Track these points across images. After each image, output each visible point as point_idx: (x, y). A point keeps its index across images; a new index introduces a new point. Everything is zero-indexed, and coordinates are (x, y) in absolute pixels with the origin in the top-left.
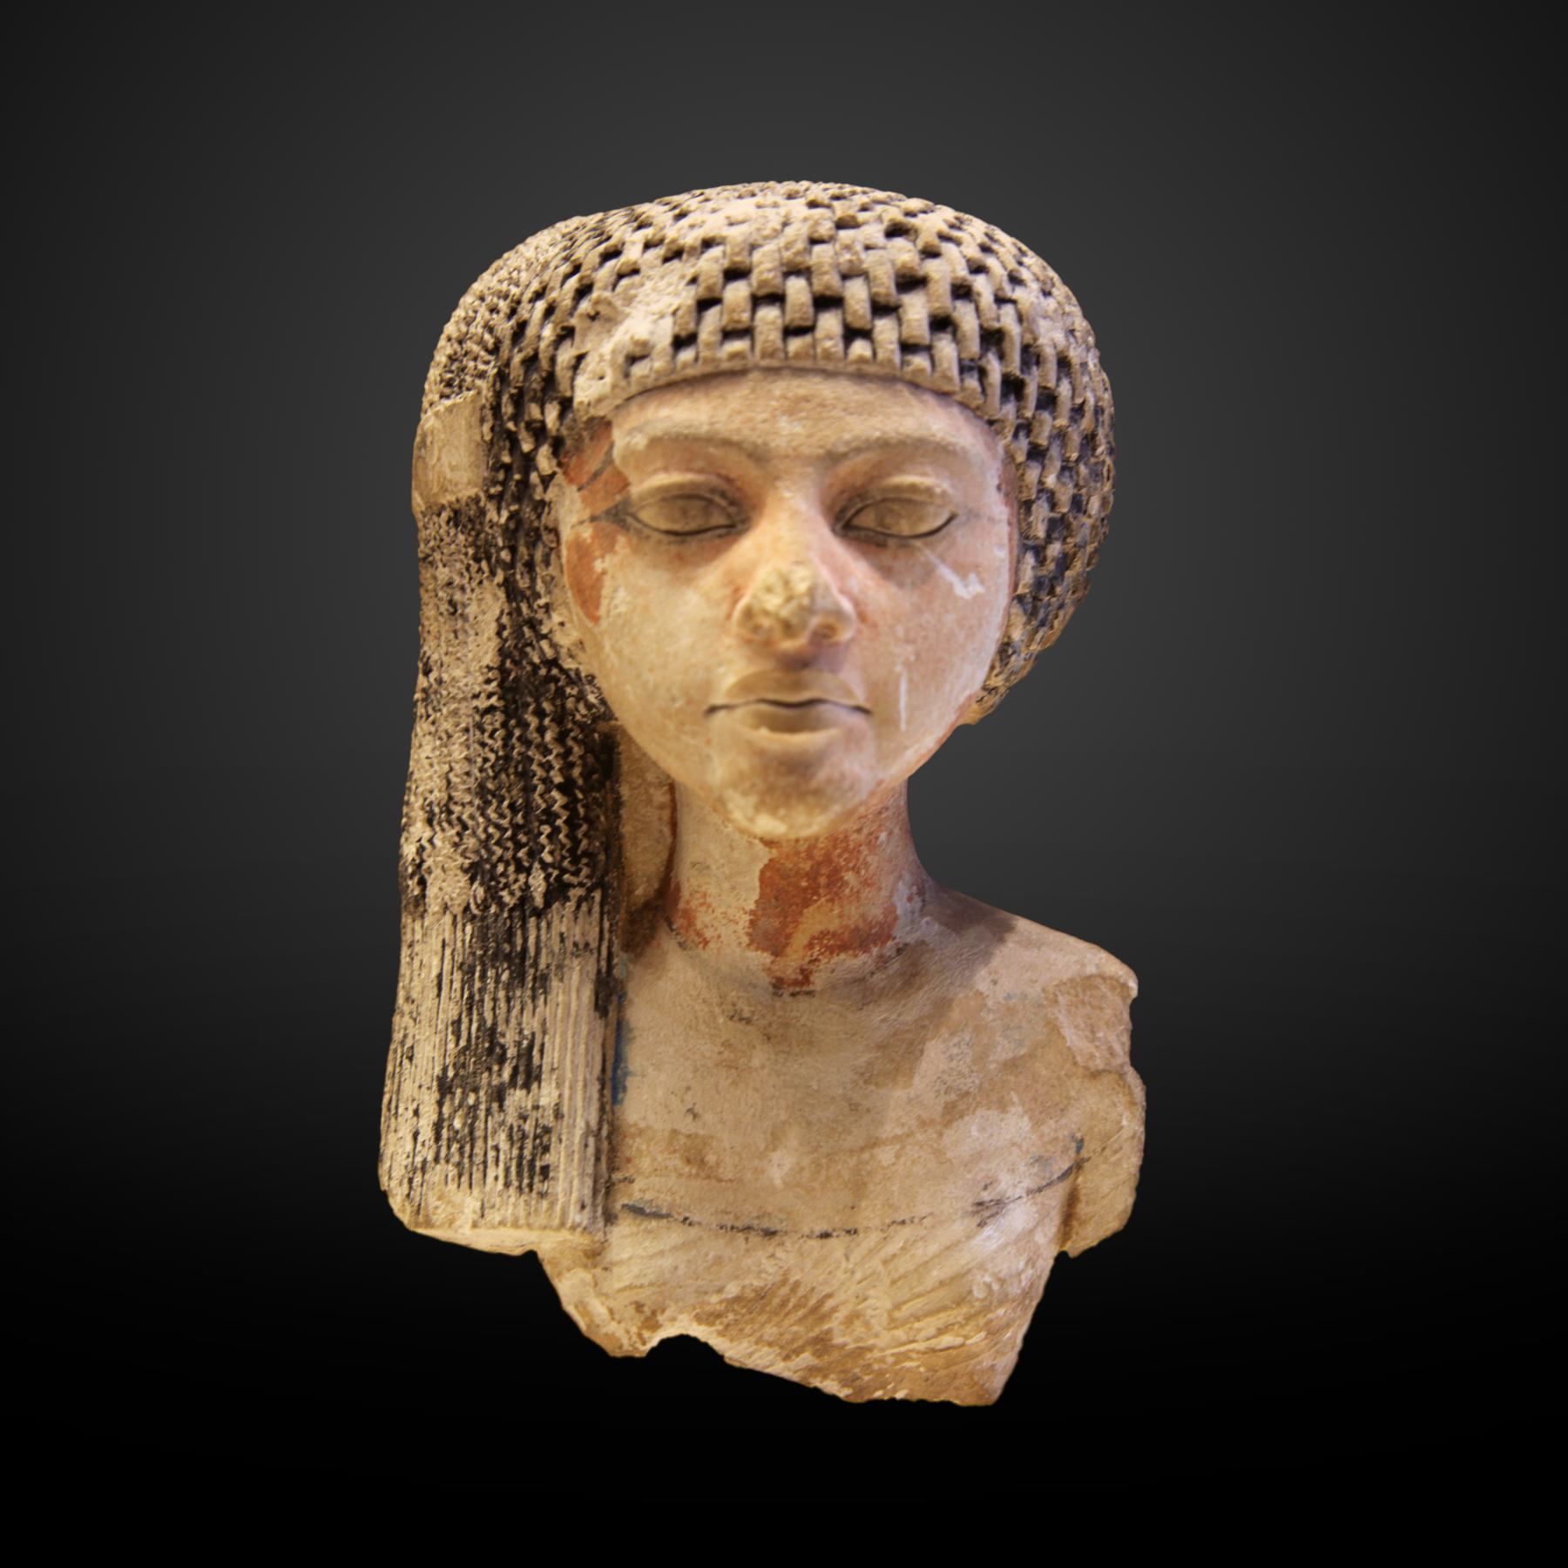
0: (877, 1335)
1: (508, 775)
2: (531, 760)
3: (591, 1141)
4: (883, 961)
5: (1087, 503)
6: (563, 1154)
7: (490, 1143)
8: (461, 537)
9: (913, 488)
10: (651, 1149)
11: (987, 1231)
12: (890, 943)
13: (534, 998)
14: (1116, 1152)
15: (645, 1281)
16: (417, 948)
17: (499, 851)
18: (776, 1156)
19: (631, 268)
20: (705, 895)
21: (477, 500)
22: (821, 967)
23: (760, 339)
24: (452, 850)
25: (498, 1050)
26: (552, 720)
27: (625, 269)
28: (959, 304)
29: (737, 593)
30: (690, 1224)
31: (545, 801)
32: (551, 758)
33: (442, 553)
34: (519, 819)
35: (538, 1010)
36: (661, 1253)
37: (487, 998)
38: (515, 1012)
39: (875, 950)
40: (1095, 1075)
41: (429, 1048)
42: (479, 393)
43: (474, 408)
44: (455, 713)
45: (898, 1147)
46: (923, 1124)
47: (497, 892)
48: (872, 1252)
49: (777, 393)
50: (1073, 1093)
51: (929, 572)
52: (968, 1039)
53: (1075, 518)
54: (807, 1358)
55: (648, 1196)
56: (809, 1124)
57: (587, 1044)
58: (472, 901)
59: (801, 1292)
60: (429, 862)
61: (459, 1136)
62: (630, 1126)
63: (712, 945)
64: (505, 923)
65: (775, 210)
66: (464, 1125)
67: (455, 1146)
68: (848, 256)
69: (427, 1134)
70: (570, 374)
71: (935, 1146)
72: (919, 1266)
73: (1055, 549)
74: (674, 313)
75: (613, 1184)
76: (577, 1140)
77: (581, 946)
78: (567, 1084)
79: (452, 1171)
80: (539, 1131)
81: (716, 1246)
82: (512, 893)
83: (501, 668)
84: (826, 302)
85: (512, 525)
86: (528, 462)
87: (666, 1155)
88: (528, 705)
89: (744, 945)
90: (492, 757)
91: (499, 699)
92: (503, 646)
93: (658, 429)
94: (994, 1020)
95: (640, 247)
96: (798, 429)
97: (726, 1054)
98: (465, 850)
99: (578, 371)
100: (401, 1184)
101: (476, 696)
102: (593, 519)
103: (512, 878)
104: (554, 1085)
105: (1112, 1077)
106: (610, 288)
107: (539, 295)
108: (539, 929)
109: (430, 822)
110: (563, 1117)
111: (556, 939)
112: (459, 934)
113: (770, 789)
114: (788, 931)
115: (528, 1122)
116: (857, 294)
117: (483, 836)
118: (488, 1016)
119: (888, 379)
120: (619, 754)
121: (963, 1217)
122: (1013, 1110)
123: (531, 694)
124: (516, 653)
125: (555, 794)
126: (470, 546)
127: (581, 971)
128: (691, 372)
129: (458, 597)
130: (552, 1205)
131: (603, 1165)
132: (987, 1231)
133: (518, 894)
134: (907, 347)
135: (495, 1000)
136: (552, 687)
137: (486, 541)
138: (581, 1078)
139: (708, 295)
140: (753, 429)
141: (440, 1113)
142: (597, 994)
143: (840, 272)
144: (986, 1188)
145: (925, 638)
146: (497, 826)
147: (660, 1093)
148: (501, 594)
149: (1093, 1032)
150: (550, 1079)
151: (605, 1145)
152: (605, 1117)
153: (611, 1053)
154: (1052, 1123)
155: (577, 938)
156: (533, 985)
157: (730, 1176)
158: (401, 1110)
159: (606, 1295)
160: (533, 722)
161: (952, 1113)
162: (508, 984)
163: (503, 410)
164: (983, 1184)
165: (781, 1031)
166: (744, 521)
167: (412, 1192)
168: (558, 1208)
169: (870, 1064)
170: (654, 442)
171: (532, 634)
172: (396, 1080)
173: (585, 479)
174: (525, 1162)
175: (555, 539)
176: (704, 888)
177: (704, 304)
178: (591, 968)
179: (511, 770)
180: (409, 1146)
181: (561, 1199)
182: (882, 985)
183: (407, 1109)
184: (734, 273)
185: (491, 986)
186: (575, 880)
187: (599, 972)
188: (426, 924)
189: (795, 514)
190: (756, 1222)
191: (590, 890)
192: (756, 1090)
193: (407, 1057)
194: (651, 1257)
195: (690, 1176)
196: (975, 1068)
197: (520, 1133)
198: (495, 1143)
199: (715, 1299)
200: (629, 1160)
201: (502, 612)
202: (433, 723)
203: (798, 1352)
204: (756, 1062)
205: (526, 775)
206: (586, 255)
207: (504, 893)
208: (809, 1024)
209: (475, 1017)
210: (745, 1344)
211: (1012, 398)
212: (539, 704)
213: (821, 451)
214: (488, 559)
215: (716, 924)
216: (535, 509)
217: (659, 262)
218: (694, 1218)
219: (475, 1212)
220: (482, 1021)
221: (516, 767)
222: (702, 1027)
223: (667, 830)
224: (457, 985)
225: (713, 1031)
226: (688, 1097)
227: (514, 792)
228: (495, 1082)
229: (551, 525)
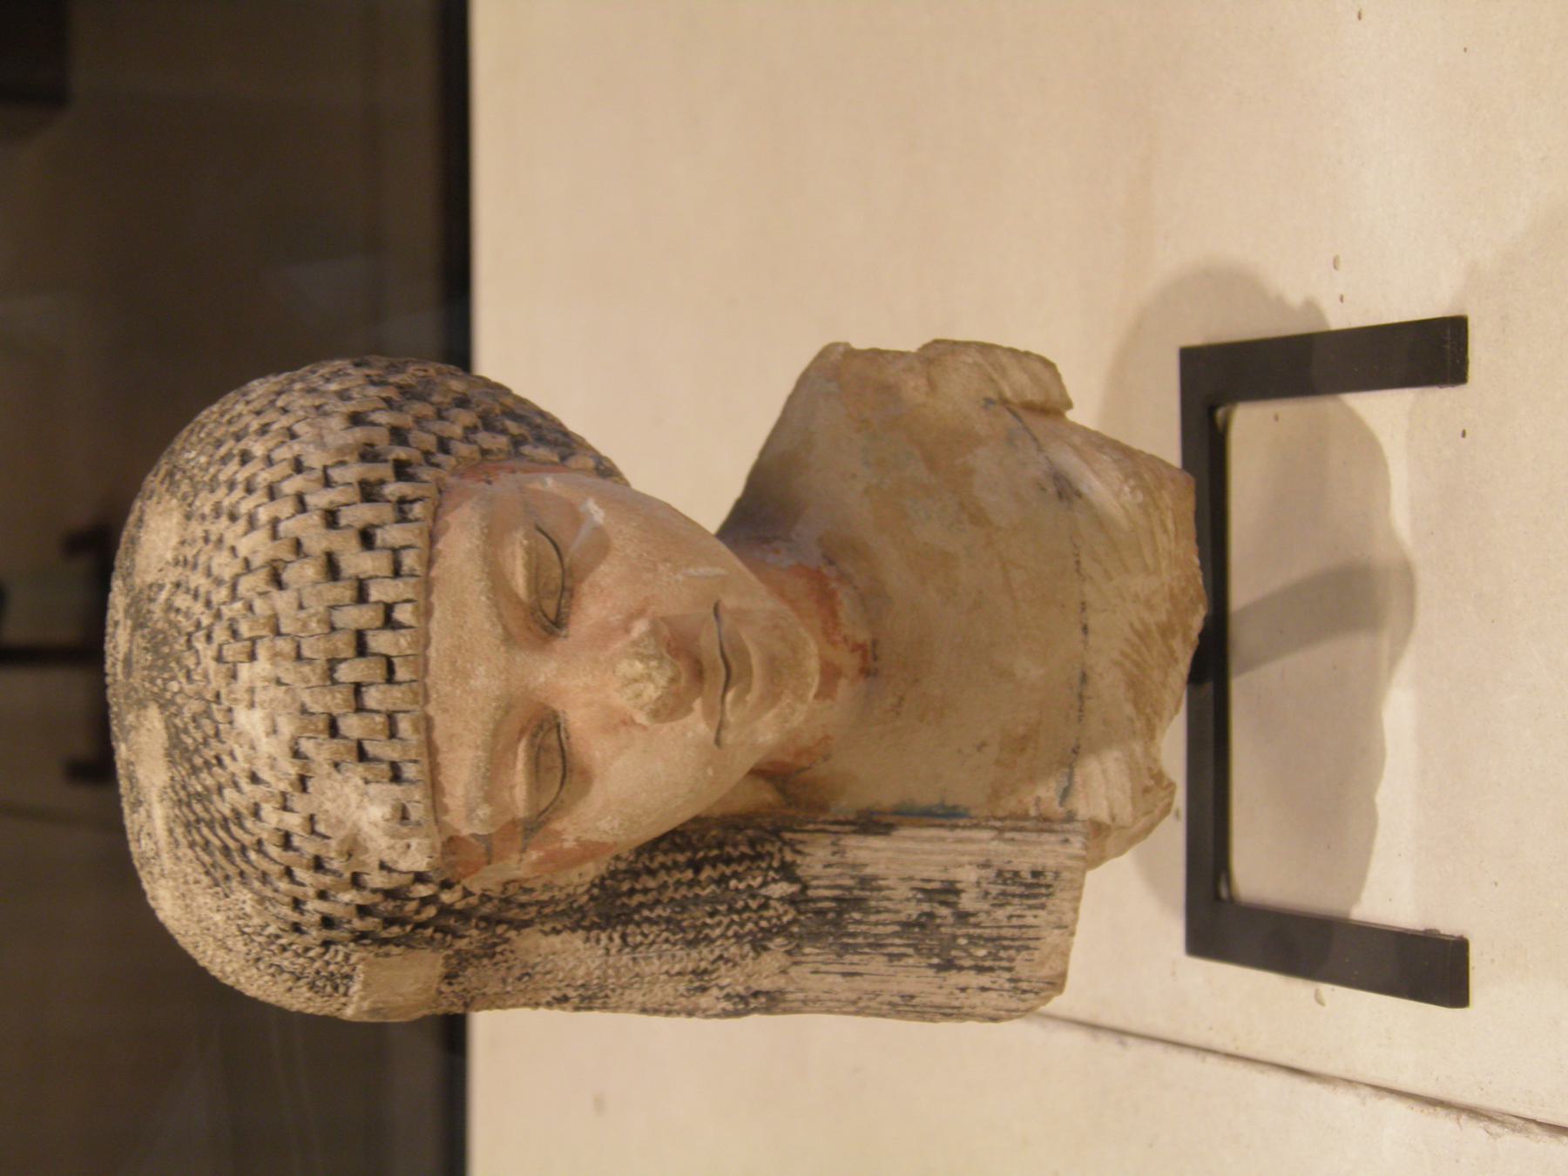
1: (684, 920)
3: (1008, 835)
4: (843, 577)
5: (456, 392)
6: (1022, 860)
8: (470, 971)
9: (527, 565)
16: (812, 995)
17: (750, 926)
21: (447, 958)
25: (923, 919)
27: (308, 829)
28: (343, 522)
29: (628, 722)
30: (1078, 747)
31: (708, 885)
34: (723, 908)
36: (1104, 772)
39: (833, 585)
49: (448, 689)
53: (478, 406)
59: (1128, 650)
60: (740, 989)
64: (810, 918)
65: (258, 690)
66: (983, 947)
67: (1002, 954)
68: (314, 625)
69: (985, 980)
70: (395, 875)
73: (513, 427)
74: (367, 782)
75: (1041, 815)
77: (835, 849)
79: (1024, 954)
80: (1000, 881)
82: (786, 912)
83: (589, 929)
85: (483, 924)
88: (624, 905)
95: (287, 816)
96: (482, 670)
99: (394, 867)
100: (1024, 1000)
102: (523, 850)
106: (326, 841)
107: (297, 904)
108: (818, 887)
109: (704, 989)
111: (829, 871)
112: (810, 959)
115: (991, 891)
116: (353, 617)
117: (733, 940)
119: (428, 586)
125: (703, 876)
128: (426, 767)
129: (517, 972)
130: (1068, 868)
131: (1027, 824)
132: (1084, 489)
133: (787, 907)
134: (397, 573)
135: (877, 924)
136: (608, 882)
137: (481, 948)
141: (970, 968)
143: (330, 633)
145: (648, 553)
146: (728, 927)
151: (1009, 823)
152: (984, 823)
158: (957, 1004)
160: (637, 899)
162: (864, 913)
168: (1069, 863)
170: (489, 798)
172: (925, 1009)
175: (512, 884)
177: (362, 756)
179: (679, 917)
180: (993, 995)
186: (778, 856)
187: (855, 832)
191: (785, 843)
193: (910, 1001)
197: (1001, 897)
198: (1006, 920)
199: (1138, 725)
203: (1171, 651)
205: (683, 905)
206: (276, 862)
207: (785, 919)
209: (889, 941)
211: (410, 470)
213: (502, 649)
214: (495, 945)
217: (305, 797)
220: (895, 934)
224: (856, 958)
227: (698, 914)
228: (951, 920)
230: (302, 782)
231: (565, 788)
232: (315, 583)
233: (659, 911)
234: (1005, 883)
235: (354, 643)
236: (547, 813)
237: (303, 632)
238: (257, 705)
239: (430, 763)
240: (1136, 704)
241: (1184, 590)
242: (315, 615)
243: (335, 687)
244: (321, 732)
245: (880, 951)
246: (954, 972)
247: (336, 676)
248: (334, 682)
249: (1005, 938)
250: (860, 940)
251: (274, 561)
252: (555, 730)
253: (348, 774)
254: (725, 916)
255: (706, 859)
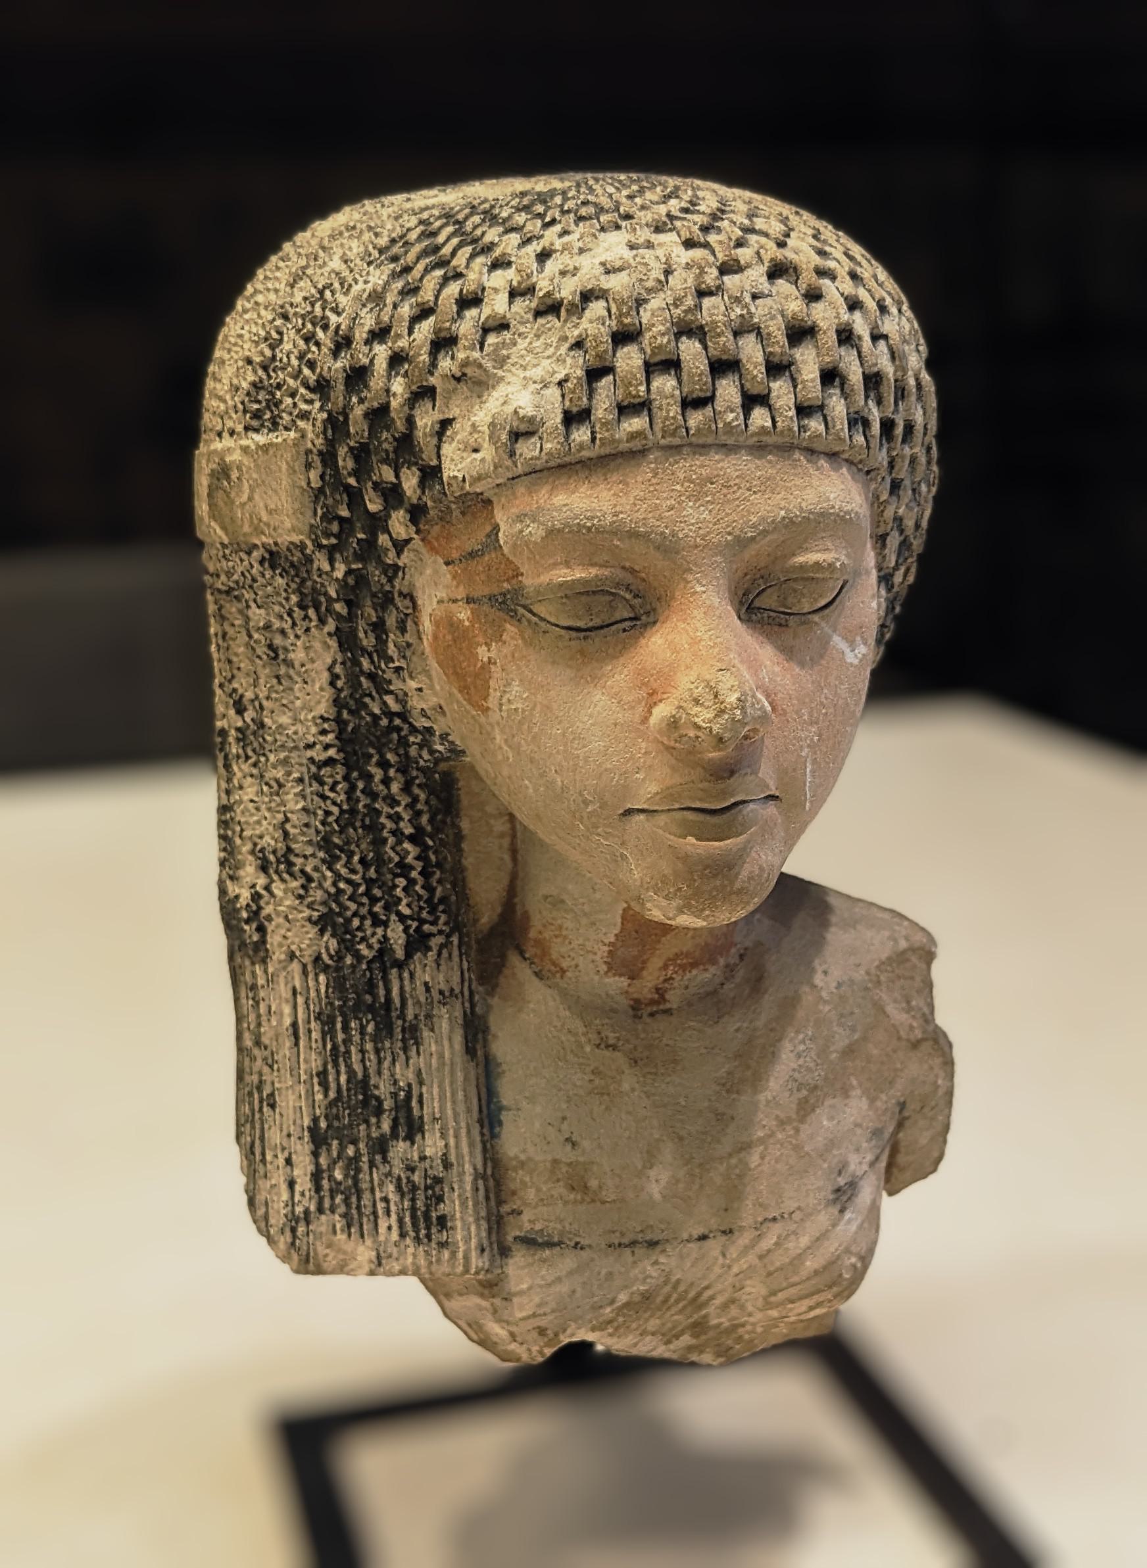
0: (750, 1315)
1: (355, 830)
2: (378, 813)
3: (480, 1182)
4: (730, 969)
6: (457, 1203)
7: (378, 1195)
10: (535, 1180)
11: (848, 1215)
12: (733, 950)
13: (405, 1049)
14: (933, 1108)
15: (547, 1309)
16: (262, 994)
17: (353, 906)
18: (652, 1173)
19: (498, 323)
20: (560, 927)
22: (676, 984)
23: (659, 416)
24: (297, 902)
26: (397, 771)
27: (491, 323)
30: (582, 1248)
31: (397, 853)
32: (399, 809)
33: (256, 594)
34: (372, 873)
35: (411, 1061)
36: (559, 1280)
37: (353, 1049)
38: (386, 1064)
40: (915, 1045)
41: (292, 1098)
42: (303, 436)
43: (298, 452)
44: (285, 762)
45: (762, 1148)
46: (782, 1123)
47: (353, 945)
48: (746, 1249)
50: (899, 1066)
51: (825, 643)
52: (810, 1033)
54: (686, 1339)
55: (538, 1227)
56: (681, 1139)
57: (465, 1091)
58: (323, 951)
59: (682, 1288)
60: (268, 910)
61: (342, 1188)
62: (512, 1159)
63: (569, 974)
64: (364, 975)
65: (651, 252)
66: (346, 1176)
67: (339, 1199)
68: (738, 311)
69: (304, 1183)
70: (435, 441)
71: (794, 1142)
72: (794, 1259)
74: (560, 384)
76: (468, 1187)
77: (447, 994)
78: (451, 1132)
81: (605, 1264)
82: (370, 947)
83: (338, 720)
84: (722, 366)
86: (378, 523)
87: (550, 1185)
88: (371, 756)
89: (602, 972)
90: (335, 810)
91: (339, 751)
92: (338, 696)
93: (558, 519)
94: (830, 1011)
95: (505, 296)
97: (597, 1081)
98: (313, 903)
101: (309, 746)
102: (469, 600)
103: (369, 932)
104: (438, 1135)
105: (931, 1043)
108: (401, 979)
109: (264, 868)
110: (452, 1165)
111: (421, 989)
112: (311, 983)
113: (697, 894)
114: (645, 957)
115: (417, 1173)
117: (332, 890)
118: (357, 1067)
120: (459, 789)
121: (826, 1206)
122: (853, 1093)
123: (371, 744)
124: (352, 702)
125: (407, 845)
126: (294, 593)
127: (450, 1018)
128: (586, 454)
130: (453, 1254)
131: (493, 1203)
133: (376, 946)
134: (803, 411)
136: (395, 736)
138: (463, 1124)
139: (597, 364)
140: (660, 518)
141: (317, 1165)
142: (466, 1038)
144: (840, 1173)
146: (349, 882)
147: (537, 1125)
148: (333, 643)
149: (908, 1002)
150: (434, 1129)
151: (491, 1183)
153: (484, 1090)
154: (884, 1097)
155: (443, 986)
156: (403, 1036)
157: (612, 1197)
158: (269, 1157)
159: (508, 1323)
160: (378, 774)
161: (805, 1109)
162: (376, 1035)
163: (341, 463)
164: (836, 1171)
165: (646, 1053)
166: (648, 613)
167: (298, 1241)
169: (729, 1073)
170: (551, 533)
171: (371, 685)
172: (257, 1126)
173: (455, 555)
174: (419, 1213)
175: (411, 605)
176: (559, 922)
177: (594, 374)
178: (458, 1013)
179: (358, 824)
180: (285, 1196)
181: (462, 1248)
182: (732, 995)
183: (276, 1156)
184: (624, 337)
185: (356, 1038)
186: (434, 929)
188: (271, 970)
189: (709, 610)
190: (641, 1235)
192: (629, 1113)
193: (268, 1105)
194: (549, 1285)
195: (575, 1202)
196: (819, 1061)
200: (514, 1193)
201: (334, 662)
202: (255, 765)
203: (677, 1337)
204: (626, 1086)
205: (373, 828)
206: (437, 298)
207: (362, 947)
208: (671, 1042)
209: (343, 1069)
210: (631, 1337)
212: (382, 755)
214: (317, 609)
215: (572, 954)
216: (385, 573)
217: (530, 316)
218: (584, 1242)
219: (371, 1261)
220: (351, 1073)
221: (363, 821)
222: (570, 1057)
223: (507, 857)
225: (581, 1060)
226: (565, 1126)
227: (364, 846)
228: (375, 1134)
229: (405, 591)
230: (551, 308)
231: (563, 632)
232: (782, 312)
233: (364, 801)
234: (427, 1188)
235: (725, 357)
236: (526, 613)
237: (730, 297)
238: (635, 252)
239: (590, 459)
240: (627, 1305)
241: (740, 1339)
242: (749, 313)
243: (673, 337)
244: (620, 322)
245: (329, 1059)
246: (312, 1147)
247: (684, 338)
248: (678, 335)
249: (359, 1199)
250: (340, 1036)
251: (795, 269)
252: (632, 615)
253: (569, 361)
254: (363, 878)
255: (425, 848)
